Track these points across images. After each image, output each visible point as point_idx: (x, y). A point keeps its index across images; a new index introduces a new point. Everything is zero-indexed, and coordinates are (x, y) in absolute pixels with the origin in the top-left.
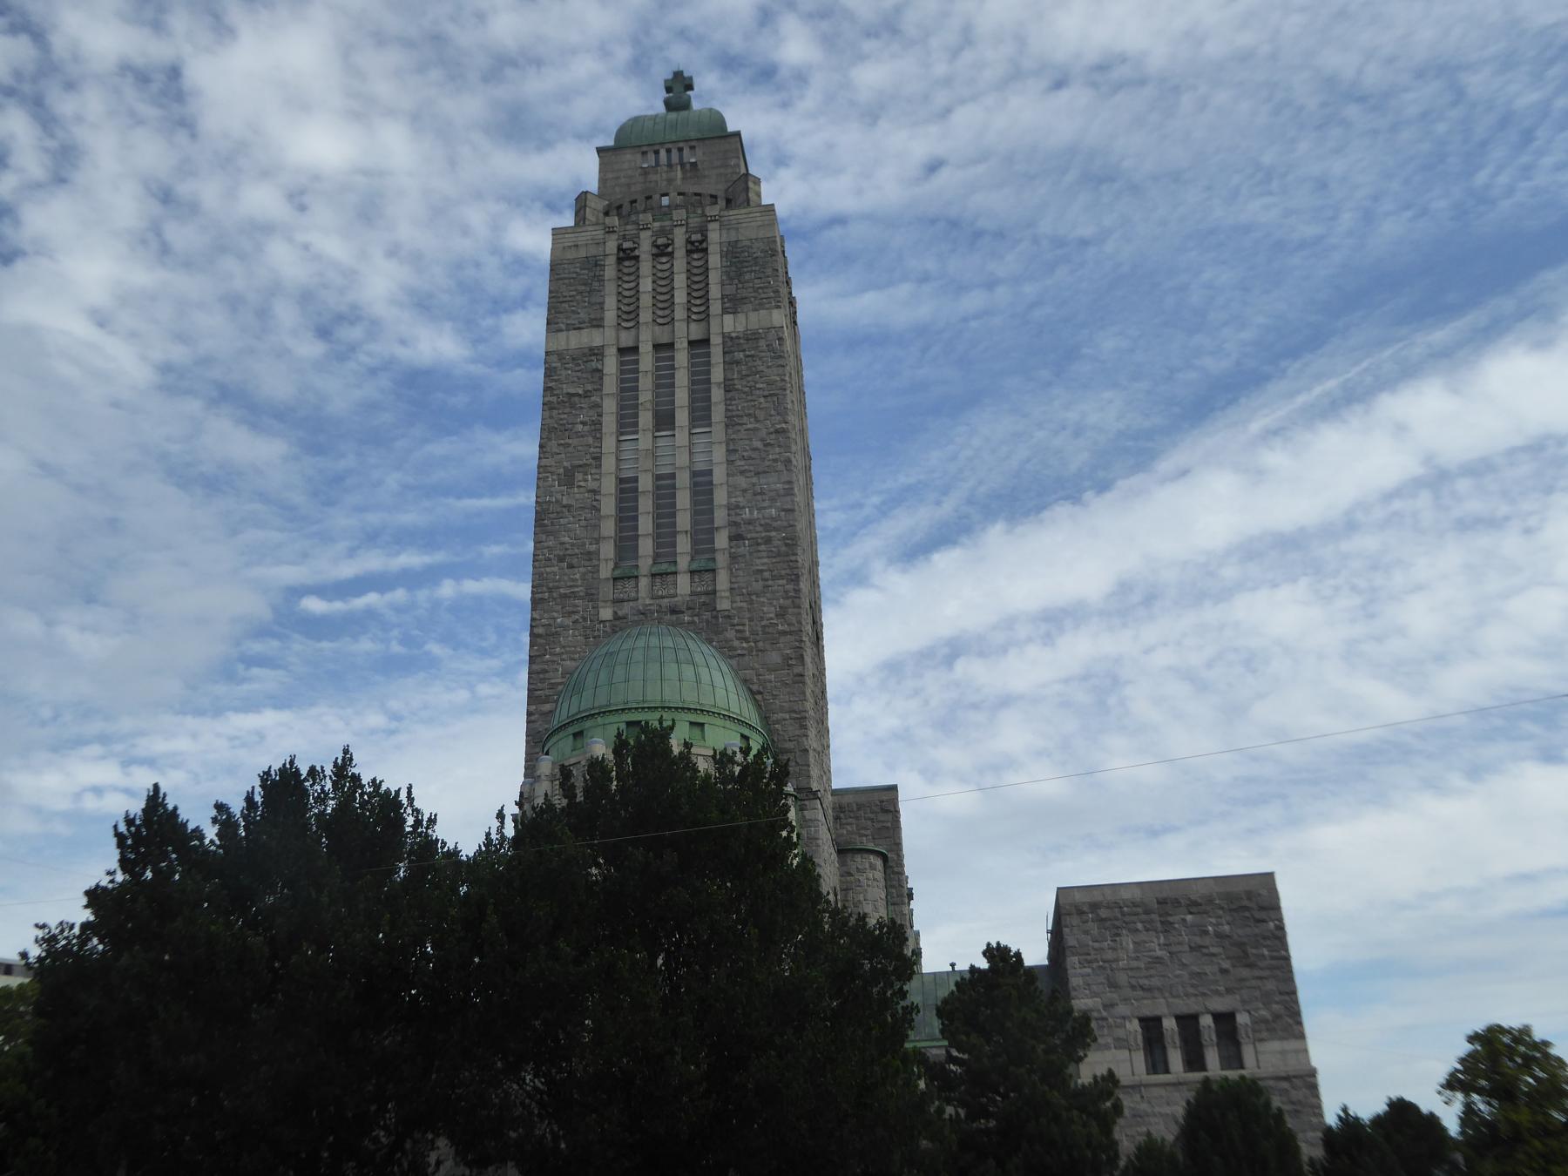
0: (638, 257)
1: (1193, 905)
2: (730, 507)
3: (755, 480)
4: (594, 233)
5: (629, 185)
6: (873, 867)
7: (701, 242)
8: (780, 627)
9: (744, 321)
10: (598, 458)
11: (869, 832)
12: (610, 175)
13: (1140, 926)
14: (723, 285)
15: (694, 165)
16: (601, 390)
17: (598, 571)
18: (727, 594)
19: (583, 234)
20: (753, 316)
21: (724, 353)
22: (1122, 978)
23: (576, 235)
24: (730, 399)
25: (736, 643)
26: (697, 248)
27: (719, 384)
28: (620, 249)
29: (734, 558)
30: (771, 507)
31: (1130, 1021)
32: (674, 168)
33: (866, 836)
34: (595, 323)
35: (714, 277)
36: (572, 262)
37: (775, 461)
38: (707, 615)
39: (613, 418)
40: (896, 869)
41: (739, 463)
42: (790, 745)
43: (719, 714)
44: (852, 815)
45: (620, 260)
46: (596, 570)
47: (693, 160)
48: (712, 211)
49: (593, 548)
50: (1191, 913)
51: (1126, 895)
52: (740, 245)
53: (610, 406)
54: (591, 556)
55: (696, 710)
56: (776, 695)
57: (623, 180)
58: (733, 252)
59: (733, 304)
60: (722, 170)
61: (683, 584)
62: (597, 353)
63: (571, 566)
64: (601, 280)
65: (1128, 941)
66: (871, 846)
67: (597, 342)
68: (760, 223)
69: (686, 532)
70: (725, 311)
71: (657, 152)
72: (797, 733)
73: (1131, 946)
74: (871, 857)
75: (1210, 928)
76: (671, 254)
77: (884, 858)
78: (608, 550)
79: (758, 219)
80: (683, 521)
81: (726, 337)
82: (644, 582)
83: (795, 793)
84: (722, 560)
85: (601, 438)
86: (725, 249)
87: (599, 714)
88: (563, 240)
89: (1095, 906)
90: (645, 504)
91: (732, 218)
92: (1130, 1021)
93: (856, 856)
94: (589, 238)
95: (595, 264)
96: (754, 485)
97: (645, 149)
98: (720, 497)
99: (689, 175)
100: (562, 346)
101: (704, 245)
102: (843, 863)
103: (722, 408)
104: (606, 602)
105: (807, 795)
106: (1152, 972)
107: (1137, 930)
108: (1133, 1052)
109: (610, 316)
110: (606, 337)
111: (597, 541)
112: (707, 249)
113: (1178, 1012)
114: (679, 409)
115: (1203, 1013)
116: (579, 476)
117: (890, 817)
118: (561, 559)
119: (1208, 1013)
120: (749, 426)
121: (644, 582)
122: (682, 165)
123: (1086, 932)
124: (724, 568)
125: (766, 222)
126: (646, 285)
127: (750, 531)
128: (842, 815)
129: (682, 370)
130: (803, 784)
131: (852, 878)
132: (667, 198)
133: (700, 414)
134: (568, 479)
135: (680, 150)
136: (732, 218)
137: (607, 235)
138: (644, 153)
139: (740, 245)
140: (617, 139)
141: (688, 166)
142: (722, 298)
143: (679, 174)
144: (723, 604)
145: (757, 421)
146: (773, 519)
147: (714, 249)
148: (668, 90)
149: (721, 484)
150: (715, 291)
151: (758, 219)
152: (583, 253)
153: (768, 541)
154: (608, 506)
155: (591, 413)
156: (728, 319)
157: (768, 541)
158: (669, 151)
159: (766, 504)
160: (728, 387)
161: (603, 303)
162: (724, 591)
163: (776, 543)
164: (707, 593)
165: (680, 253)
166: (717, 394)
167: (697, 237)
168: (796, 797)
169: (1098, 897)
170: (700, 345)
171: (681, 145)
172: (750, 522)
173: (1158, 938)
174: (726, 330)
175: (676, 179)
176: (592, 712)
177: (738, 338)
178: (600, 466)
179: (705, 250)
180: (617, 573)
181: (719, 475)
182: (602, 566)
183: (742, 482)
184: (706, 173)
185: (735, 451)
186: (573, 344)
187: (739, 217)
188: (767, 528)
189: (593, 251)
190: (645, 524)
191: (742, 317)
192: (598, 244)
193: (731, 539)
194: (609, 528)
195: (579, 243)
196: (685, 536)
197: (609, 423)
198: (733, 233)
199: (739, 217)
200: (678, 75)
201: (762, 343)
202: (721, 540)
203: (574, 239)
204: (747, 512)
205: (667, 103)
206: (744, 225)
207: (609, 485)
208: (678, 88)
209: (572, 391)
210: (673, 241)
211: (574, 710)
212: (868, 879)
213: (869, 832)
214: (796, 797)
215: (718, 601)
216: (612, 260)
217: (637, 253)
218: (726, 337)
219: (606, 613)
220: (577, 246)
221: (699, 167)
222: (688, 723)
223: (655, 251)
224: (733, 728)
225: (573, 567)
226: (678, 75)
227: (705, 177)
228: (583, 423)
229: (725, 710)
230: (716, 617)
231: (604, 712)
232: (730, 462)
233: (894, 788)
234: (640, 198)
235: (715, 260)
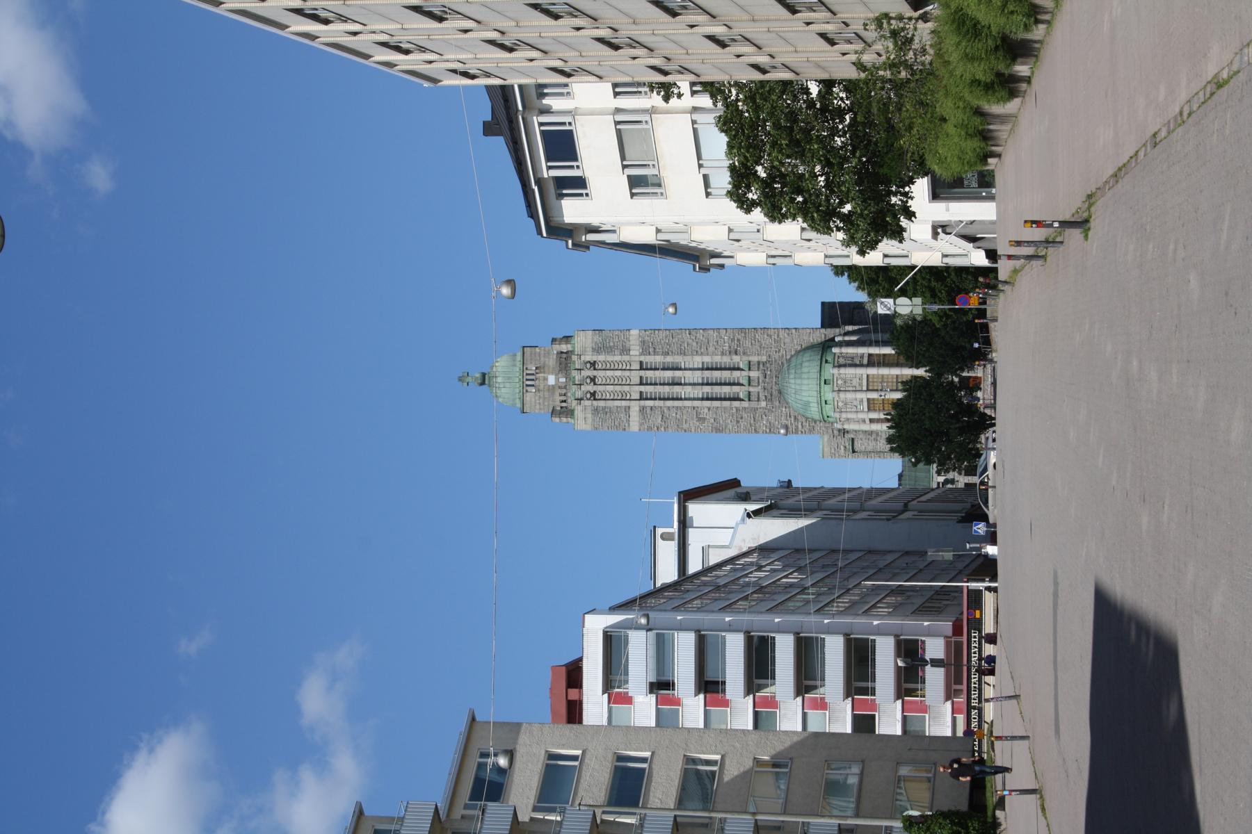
2: (723, 354)
3: (711, 344)
5: (544, 398)
7: (591, 364)
8: (776, 337)
10: (694, 408)
14: (614, 355)
15: (537, 368)
16: (661, 407)
18: (760, 357)
20: (631, 343)
21: (649, 354)
24: (672, 352)
25: (780, 354)
26: (593, 365)
28: (589, 399)
30: (724, 339)
34: (627, 410)
35: (610, 358)
36: (594, 420)
37: (703, 336)
38: (768, 365)
41: (702, 350)
45: (595, 399)
47: (534, 368)
48: (574, 358)
49: (734, 410)
52: (594, 347)
53: (669, 403)
54: (737, 409)
57: (541, 401)
58: (597, 350)
59: (625, 350)
60: (542, 356)
61: (754, 374)
62: (642, 409)
63: (742, 418)
64: (604, 408)
67: (637, 409)
71: (527, 385)
76: (595, 377)
78: (736, 404)
81: (641, 354)
82: (751, 389)
95: (596, 411)
96: (713, 345)
97: (525, 391)
98: (718, 359)
99: (542, 371)
103: (676, 357)
109: (624, 403)
110: (635, 407)
111: (731, 409)
116: (701, 416)
120: (686, 346)
121: (751, 389)
122: (537, 373)
127: (734, 347)
134: (702, 420)
138: (527, 391)
139: (594, 347)
141: (538, 371)
143: (540, 375)
144: (764, 359)
145: (684, 342)
146: (730, 337)
147: (594, 358)
150: (618, 358)
152: (589, 415)
155: (671, 410)
156: (632, 353)
157: (738, 340)
158: (527, 380)
159: (722, 340)
163: (740, 337)
164: (759, 365)
165: (595, 373)
166: (669, 359)
167: (588, 365)
171: (525, 374)
172: (730, 347)
174: (638, 353)
175: (544, 377)
177: (643, 349)
178: (698, 407)
179: (595, 362)
180: (746, 399)
181: (707, 359)
182: (743, 406)
183: (711, 349)
184: (542, 363)
185: (697, 352)
188: (733, 340)
191: (632, 347)
193: (736, 354)
197: (677, 403)
201: (646, 338)
207: (707, 403)
209: (660, 419)
211: (816, 405)
216: (595, 403)
218: (641, 354)
219: (763, 404)
220: (585, 418)
221: (538, 365)
223: (592, 383)
226: (461, 379)
228: (676, 414)
232: (702, 354)
233: (823, 304)
234: (559, 391)
235: (601, 358)
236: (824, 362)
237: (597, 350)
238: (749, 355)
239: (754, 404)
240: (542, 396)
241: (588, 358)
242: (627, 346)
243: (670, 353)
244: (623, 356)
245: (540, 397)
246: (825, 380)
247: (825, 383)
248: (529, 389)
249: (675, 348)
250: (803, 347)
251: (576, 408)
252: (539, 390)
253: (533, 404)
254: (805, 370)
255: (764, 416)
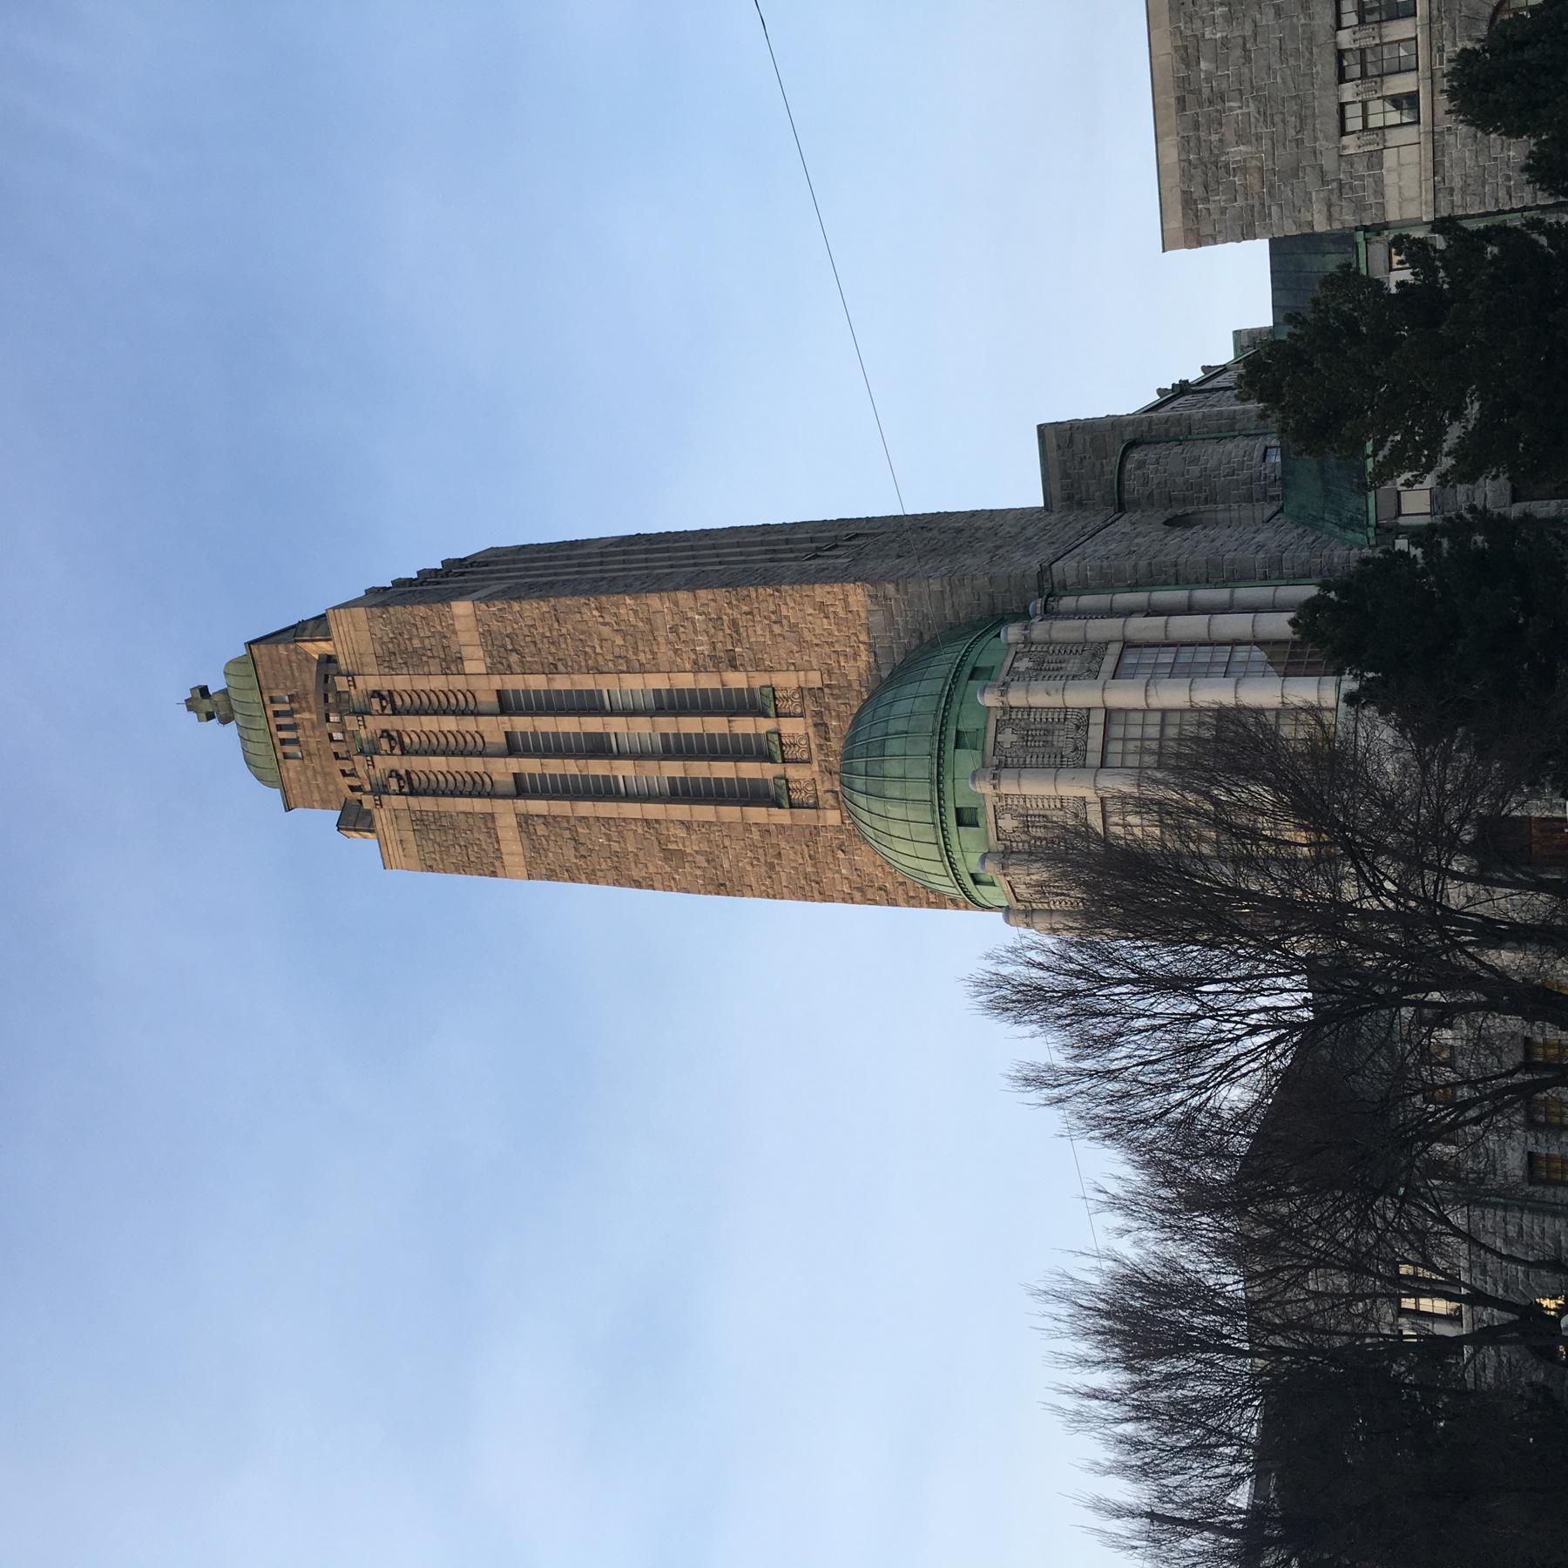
0: (406, 771)
1: (1187, 54)
2: (697, 668)
3: (661, 640)
4: (384, 821)
6: (1141, 465)
9: (470, 649)
11: (1098, 464)
12: (316, 796)
13: (1214, 137)
16: (567, 818)
17: (782, 825)
19: (387, 834)
20: (464, 638)
22: (1285, 155)
23: (388, 842)
24: (566, 666)
27: (549, 680)
29: (758, 665)
31: (1344, 148)
32: (297, 721)
33: (1102, 464)
35: (422, 684)
39: (600, 804)
40: (1145, 428)
42: (985, 599)
43: (945, 710)
44: (1076, 485)
46: (781, 828)
50: (1198, 63)
51: (1172, 156)
52: (380, 652)
53: (585, 808)
54: (765, 831)
55: (940, 741)
56: (923, 615)
57: (320, 781)
58: (389, 660)
59: (452, 663)
61: (792, 728)
62: (525, 821)
65: (1236, 152)
66: (1116, 460)
67: (512, 821)
68: (351, 626)
69: (729, 721)
70: (462, 673)
71: (283, 742)
72: (968, 590)
73: (1242, 148)
74: (1129, 466)
75: (1219, 35)
77: (1132, 445)
78: (757, 814)
79: (346, 629)
80: (716, 725)
82: (793, 772)
83: (1045, 597)
84: (760, 680)
85: (624, 819)
86: (387, 670)
87: (949, 857)
88: (397, 857)
89: (1188, 201)
90: (700, 770)
91: (348, 661)
92: (1344, 148)
93: (1127, 487)
94: (391, 828)
95: (421, 823)
98: (685, 681)
100: (519, 860)
101: (385, 693)
102: (1137, 504)
103: (576, 677)
104: (818, 818)
105: (1047, 581)
106: (1277, 118)
107: (1220, 140)
108: (1388, 144)
109: (479, 805)
111: (747, 828)
112: (389, 691)
113: (1335, 79)
114: (583, 728)
115: (1336, 43)
117: (1078, 438)
118: (772, 866)
119: (1335, 37)
123: (1223, 211)
124: (771, 678)
125: (350, 620)
126: (439, 763)
128: (1077, 497)
129: (536, 723)
130: (1032, 582)
131: (1155, 492)
132: (334, 735)
133: (589, 705)
134: (674, 856)
135: (277, 714)
136: (348, 661)
137: (385, 807)
139: (380, 652)
140: (270, 784)
141: (295, 706)
142: (446, 674)
144: (815, 679)
147: (385, 684)
148: (210, 716)
149: (669, 679)
150: (438, 683)
151: (346, 629)
153: (734, 623)
154: (705, 812)
156: (470, 667)
157: (734, 623)
158: (280, 728)
160: (552, 670)
161: (465, 813)
162: (798, 678)
163: (736, 614)
166: (561, 683)
168: (1049, 596)
169: (1175, 200)
170: (506, 705)
171: (270, 714)
173: (1231, 109)
176: (948, 864)
178: (657, 821)
181: (658, 682)
182: (776, 820)
183: (665, 653)
186: (517, 848)
187: (346, 652)
189: (405, 823)
190: (723, 770)
191: (466, 652)
192: (396, 818)
193: (735, 668)
194: (730, 813)
195: (398, 839)
196: (733, 724)
198: (366, 659)
199: (346, 652)
200: (191, 705)
201: (495, 625)
202: (737, 680)
203: (394, 843)
204: (701, 648)
205: (225, 720)
206: (356, 647)
207: (680, 811)
208: (206, 705)
210: (383, 731)
212: (1157, 471)
213: (1098, 464)
214: (1049, 596)
215: (811, 686)
216: (414, 802)
217: (402, 772)
219: (833, 817)
222: (957, 750)
224: (962, 689)
225: (780, 853)
226: (191, 705)
227: (304, 686)
229: (940, 701)
230: (828, 686)
231: (947, 851)
234: (339, 765)
236: (950, 745)
237: (389, 660)
238: (770, 670)
239: (805, 816)
240: (319, 768)
241: (373, 683)
242: (454, 648)
243: (561, 668)
244: (450, 677)
245: (315, 771)
246: (958, 811)
247: (960, 823)
248: (289, 749)
249: (568, 649)
250: (926, 637)
251: (375, 812)
252: (309, 754)
253: (306, 788)
254: (893, 767)
255: (841, 855)
